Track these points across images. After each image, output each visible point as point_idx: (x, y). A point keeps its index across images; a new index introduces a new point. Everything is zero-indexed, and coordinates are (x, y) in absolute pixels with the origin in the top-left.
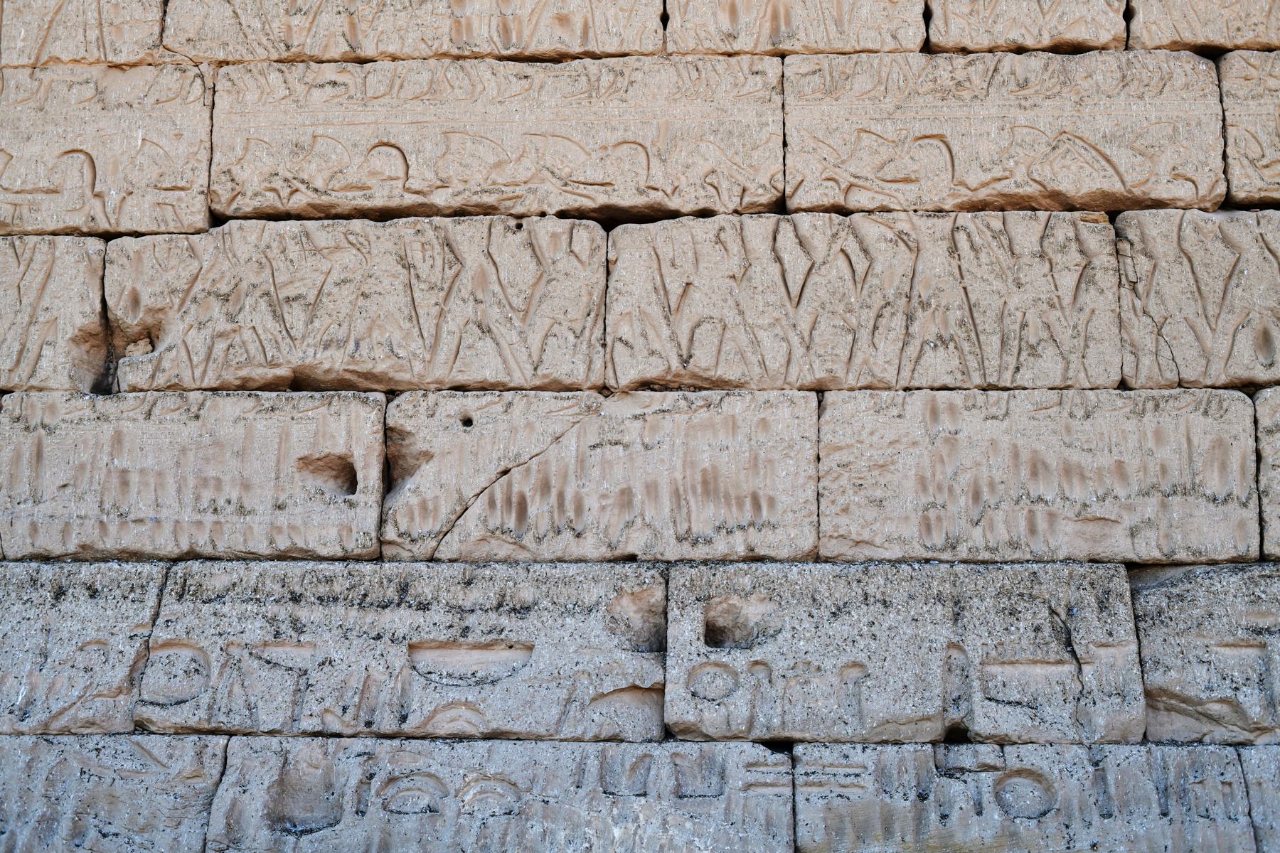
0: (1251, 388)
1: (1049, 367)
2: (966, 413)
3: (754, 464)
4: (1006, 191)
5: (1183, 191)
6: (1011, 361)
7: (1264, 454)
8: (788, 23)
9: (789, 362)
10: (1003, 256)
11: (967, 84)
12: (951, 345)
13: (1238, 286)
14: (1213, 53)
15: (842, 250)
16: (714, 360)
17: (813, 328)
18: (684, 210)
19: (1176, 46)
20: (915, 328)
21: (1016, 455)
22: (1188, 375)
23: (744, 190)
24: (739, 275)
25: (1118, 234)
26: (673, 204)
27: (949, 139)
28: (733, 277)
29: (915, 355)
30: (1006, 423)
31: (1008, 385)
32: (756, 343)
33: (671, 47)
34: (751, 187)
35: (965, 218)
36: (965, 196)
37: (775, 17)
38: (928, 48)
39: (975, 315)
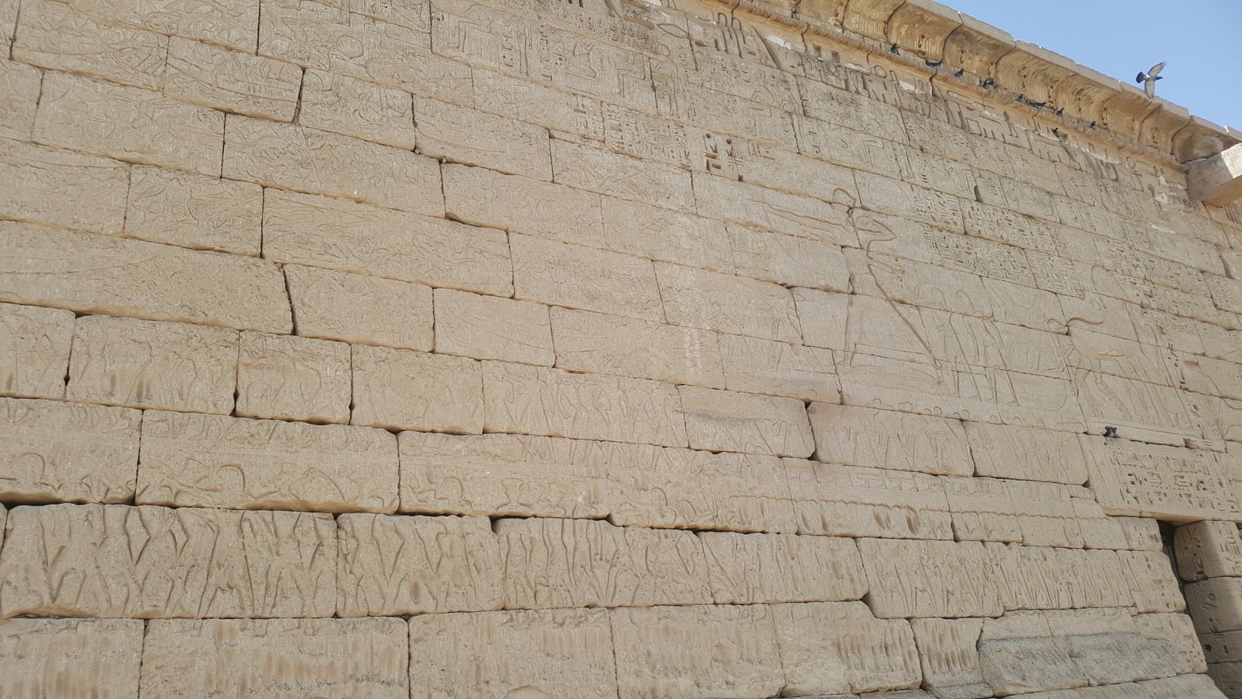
0: (406, 617)
1: (294, 604)
2: (241, 633)
3: (96, 668)
4: (275, 499)
5: (376, 504)
6: (270, 600)
7: (413, 655)
8: (148, 391)
9: (127, 600)
10: (271, 538)
11: (257, 436)
12: (235, 590)
13: (402, 557)
14: (396, 432)
15: (170, 530)
16: (74, 600)
17: (146, 578)
18: (66, 500)
19: (376, 427)
20: (212, 580)
21: (270, 659)
22: (374, 609)
23: (108, 490)
24: (99, 543)
25: (338, 527)
26: (59, 495)
27: (243, 467)
28: (95, 544)
29: (210, 597)
30: (265, 640)
31: (268, 616)
32: (106, 586)
33: (69, 397)
34: (114, 488)
35: (249, 514)
36: (251, 501)
37: (140, 387)
38: (234, 413)
39: (251, 572)
